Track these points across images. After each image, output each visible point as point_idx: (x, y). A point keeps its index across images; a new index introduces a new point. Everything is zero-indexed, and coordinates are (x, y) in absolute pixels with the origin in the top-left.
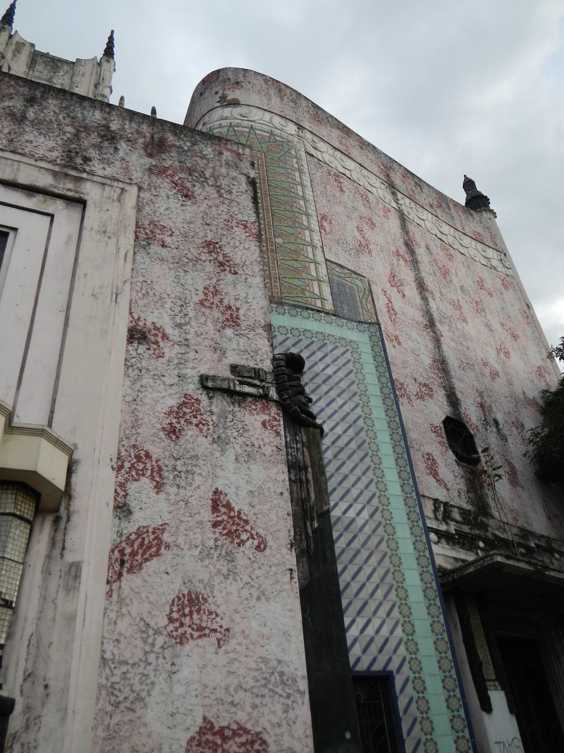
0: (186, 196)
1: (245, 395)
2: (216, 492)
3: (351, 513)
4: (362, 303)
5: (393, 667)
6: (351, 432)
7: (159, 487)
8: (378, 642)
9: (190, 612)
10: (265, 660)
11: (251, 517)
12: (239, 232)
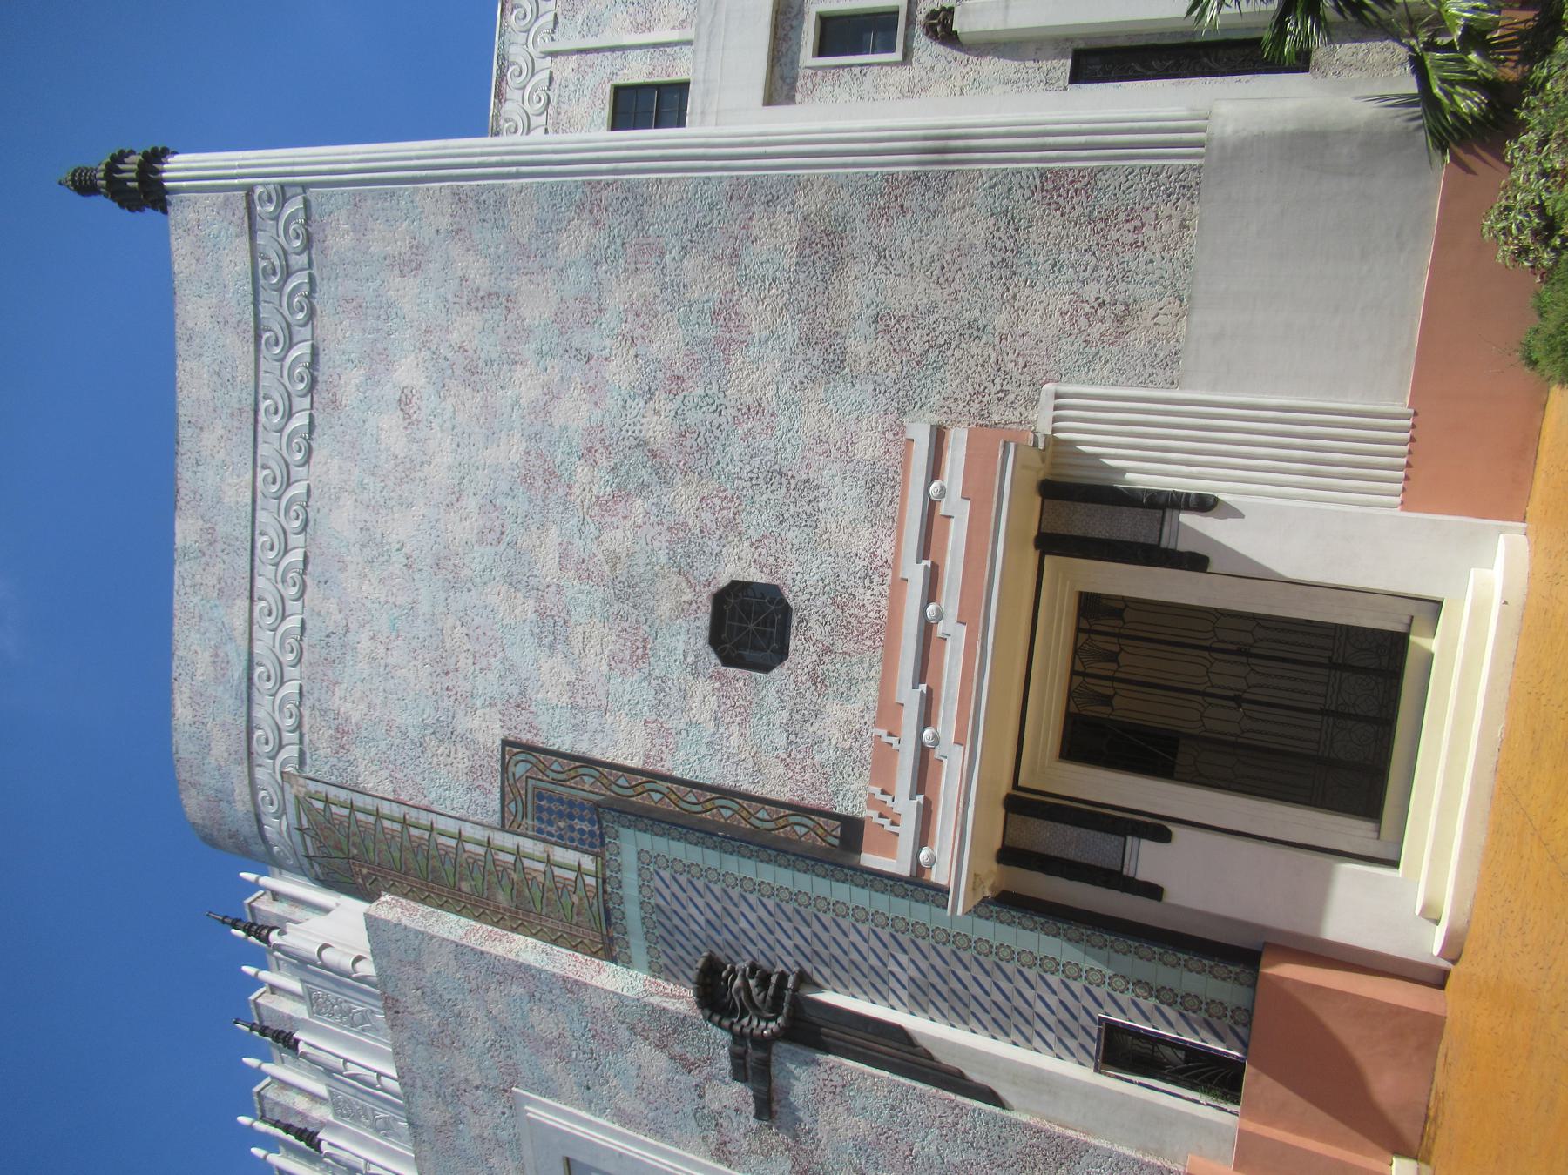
6: (785, 924)
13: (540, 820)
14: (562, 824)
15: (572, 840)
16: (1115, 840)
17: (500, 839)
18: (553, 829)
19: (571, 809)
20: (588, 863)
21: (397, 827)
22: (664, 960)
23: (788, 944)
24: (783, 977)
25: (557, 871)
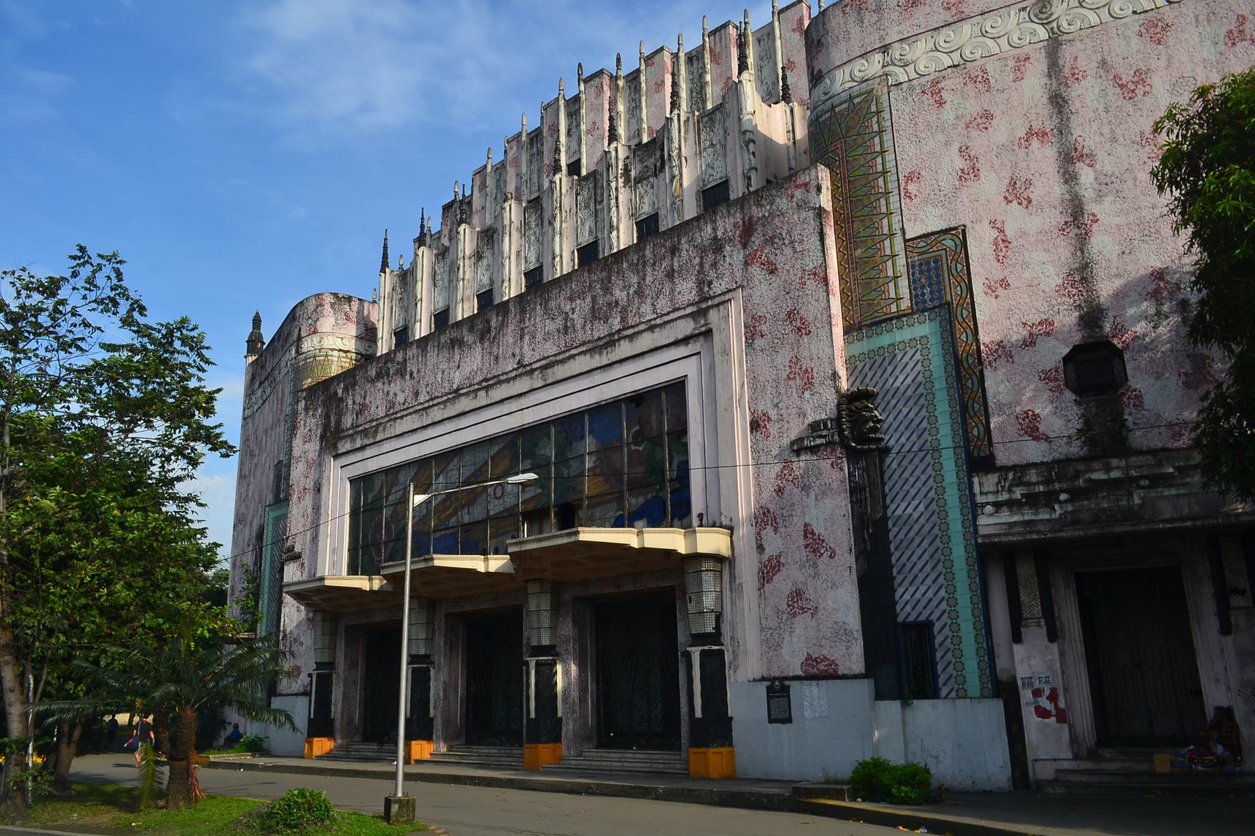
0: (772, 272)
1: (818, 446)
2: (806, 525)
3: (910, 510)
4: (949, 269)
5: (934, 618)
6: (914, 437)
7: (776, 530)
8: (924, 602)
9: (798, 600)
10: (836, 623)
11: (826, 537)
12: (811, 284)
13: (921, 265)
14: (923, 280)
15: (915, 289)
16: (1038, 611)
17: (898, 240)
18: (917, 275)
19: (937, 285)
20: (905, 304)
21: (880, 168)
22: (860, 366)
23: (903, 439)
24: (882, 439)
25: (892, 285)
